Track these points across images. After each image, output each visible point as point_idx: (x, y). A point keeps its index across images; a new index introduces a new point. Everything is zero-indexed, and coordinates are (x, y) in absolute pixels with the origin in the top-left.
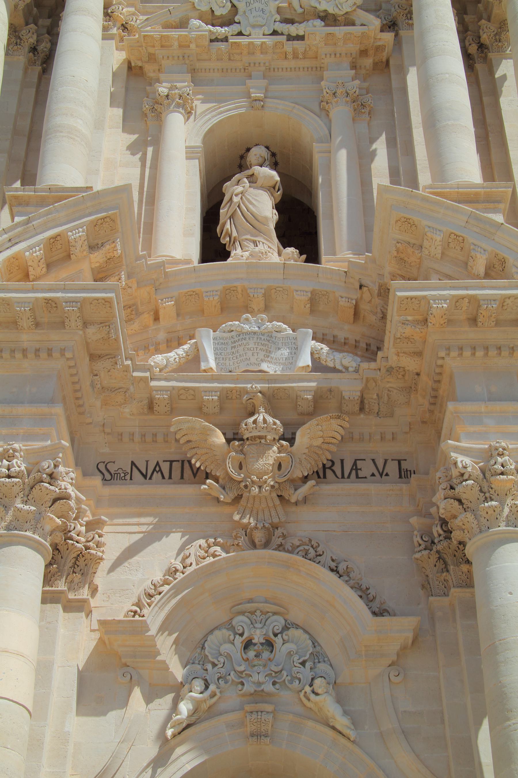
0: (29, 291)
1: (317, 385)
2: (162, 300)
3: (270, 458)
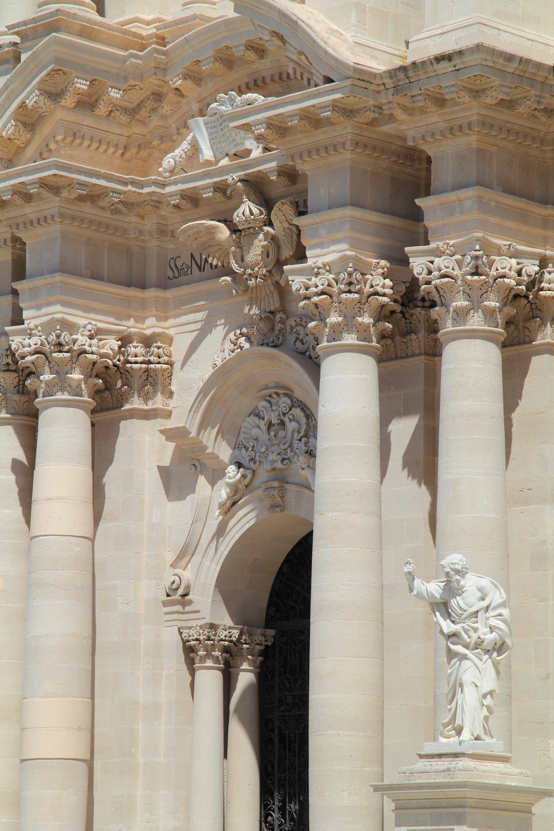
0: (6, 179)
1: (277, 163)
2: (172, 80)
3: (257, 248)
